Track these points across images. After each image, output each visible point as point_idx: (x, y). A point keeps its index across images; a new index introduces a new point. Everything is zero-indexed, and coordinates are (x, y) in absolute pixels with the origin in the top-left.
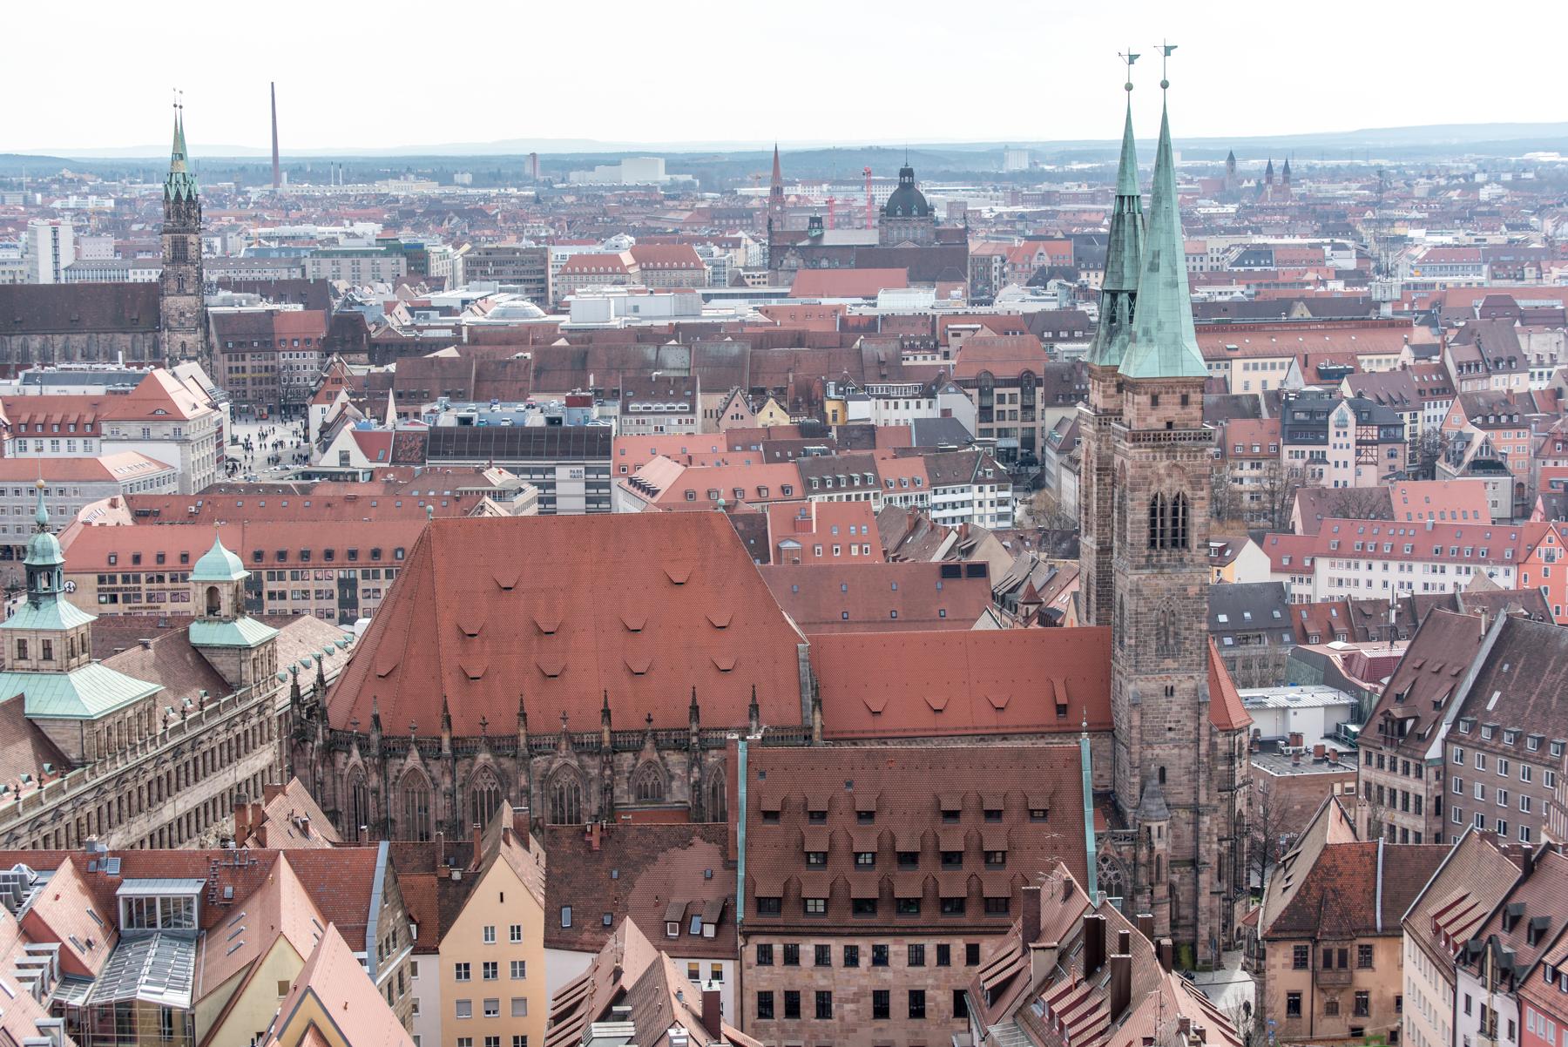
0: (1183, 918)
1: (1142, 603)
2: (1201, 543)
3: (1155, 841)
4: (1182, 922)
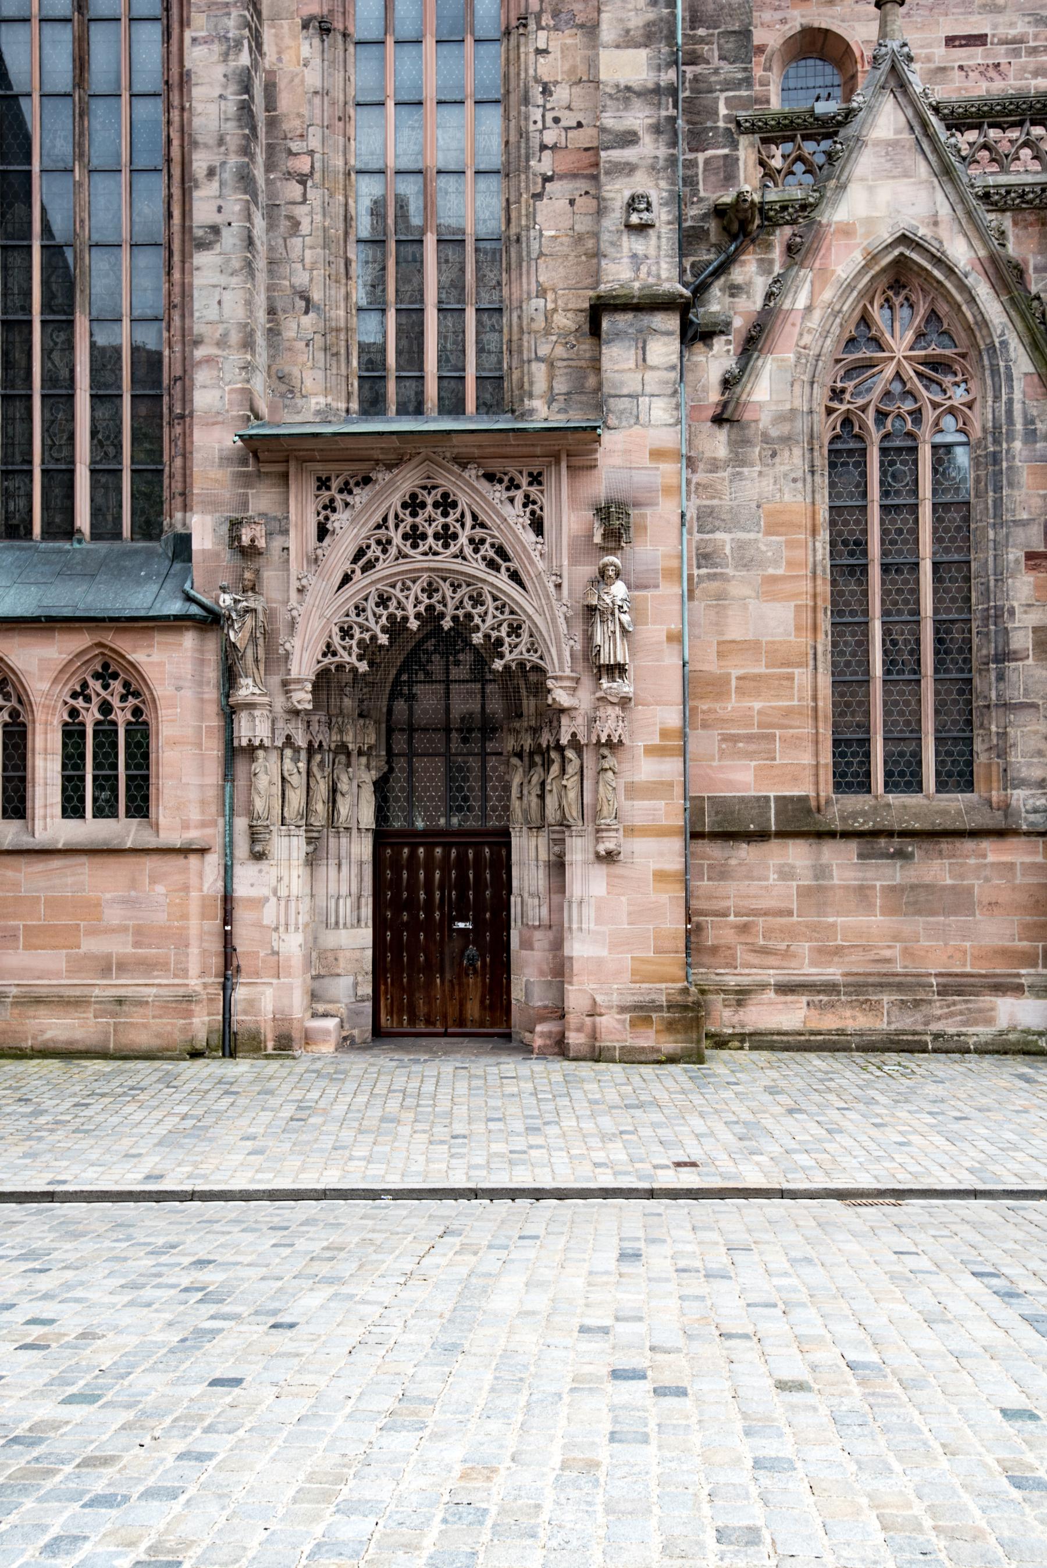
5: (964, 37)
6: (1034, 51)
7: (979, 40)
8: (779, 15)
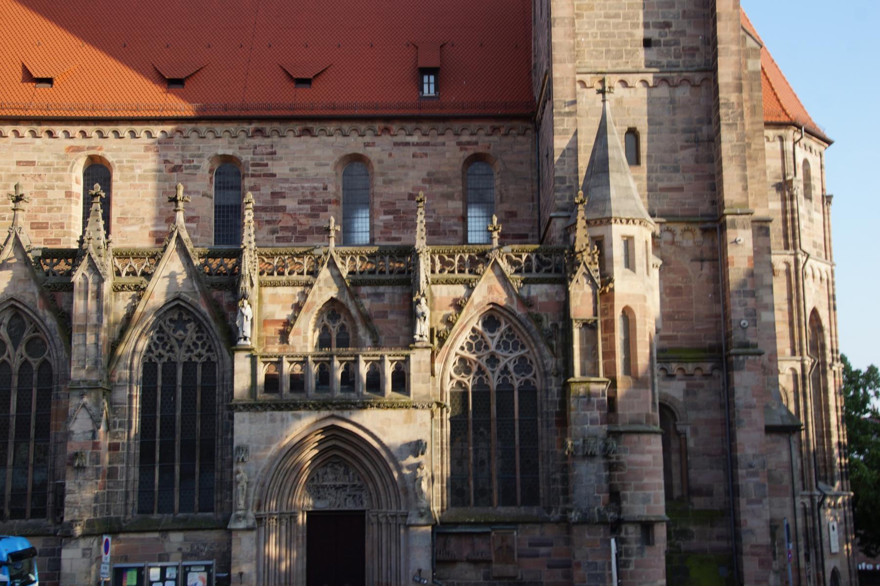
0: (699, 492)
3: (618, 269)
4: (699, 502)
5: (25, 162)
6: (56, 170)
7: (32, 163)
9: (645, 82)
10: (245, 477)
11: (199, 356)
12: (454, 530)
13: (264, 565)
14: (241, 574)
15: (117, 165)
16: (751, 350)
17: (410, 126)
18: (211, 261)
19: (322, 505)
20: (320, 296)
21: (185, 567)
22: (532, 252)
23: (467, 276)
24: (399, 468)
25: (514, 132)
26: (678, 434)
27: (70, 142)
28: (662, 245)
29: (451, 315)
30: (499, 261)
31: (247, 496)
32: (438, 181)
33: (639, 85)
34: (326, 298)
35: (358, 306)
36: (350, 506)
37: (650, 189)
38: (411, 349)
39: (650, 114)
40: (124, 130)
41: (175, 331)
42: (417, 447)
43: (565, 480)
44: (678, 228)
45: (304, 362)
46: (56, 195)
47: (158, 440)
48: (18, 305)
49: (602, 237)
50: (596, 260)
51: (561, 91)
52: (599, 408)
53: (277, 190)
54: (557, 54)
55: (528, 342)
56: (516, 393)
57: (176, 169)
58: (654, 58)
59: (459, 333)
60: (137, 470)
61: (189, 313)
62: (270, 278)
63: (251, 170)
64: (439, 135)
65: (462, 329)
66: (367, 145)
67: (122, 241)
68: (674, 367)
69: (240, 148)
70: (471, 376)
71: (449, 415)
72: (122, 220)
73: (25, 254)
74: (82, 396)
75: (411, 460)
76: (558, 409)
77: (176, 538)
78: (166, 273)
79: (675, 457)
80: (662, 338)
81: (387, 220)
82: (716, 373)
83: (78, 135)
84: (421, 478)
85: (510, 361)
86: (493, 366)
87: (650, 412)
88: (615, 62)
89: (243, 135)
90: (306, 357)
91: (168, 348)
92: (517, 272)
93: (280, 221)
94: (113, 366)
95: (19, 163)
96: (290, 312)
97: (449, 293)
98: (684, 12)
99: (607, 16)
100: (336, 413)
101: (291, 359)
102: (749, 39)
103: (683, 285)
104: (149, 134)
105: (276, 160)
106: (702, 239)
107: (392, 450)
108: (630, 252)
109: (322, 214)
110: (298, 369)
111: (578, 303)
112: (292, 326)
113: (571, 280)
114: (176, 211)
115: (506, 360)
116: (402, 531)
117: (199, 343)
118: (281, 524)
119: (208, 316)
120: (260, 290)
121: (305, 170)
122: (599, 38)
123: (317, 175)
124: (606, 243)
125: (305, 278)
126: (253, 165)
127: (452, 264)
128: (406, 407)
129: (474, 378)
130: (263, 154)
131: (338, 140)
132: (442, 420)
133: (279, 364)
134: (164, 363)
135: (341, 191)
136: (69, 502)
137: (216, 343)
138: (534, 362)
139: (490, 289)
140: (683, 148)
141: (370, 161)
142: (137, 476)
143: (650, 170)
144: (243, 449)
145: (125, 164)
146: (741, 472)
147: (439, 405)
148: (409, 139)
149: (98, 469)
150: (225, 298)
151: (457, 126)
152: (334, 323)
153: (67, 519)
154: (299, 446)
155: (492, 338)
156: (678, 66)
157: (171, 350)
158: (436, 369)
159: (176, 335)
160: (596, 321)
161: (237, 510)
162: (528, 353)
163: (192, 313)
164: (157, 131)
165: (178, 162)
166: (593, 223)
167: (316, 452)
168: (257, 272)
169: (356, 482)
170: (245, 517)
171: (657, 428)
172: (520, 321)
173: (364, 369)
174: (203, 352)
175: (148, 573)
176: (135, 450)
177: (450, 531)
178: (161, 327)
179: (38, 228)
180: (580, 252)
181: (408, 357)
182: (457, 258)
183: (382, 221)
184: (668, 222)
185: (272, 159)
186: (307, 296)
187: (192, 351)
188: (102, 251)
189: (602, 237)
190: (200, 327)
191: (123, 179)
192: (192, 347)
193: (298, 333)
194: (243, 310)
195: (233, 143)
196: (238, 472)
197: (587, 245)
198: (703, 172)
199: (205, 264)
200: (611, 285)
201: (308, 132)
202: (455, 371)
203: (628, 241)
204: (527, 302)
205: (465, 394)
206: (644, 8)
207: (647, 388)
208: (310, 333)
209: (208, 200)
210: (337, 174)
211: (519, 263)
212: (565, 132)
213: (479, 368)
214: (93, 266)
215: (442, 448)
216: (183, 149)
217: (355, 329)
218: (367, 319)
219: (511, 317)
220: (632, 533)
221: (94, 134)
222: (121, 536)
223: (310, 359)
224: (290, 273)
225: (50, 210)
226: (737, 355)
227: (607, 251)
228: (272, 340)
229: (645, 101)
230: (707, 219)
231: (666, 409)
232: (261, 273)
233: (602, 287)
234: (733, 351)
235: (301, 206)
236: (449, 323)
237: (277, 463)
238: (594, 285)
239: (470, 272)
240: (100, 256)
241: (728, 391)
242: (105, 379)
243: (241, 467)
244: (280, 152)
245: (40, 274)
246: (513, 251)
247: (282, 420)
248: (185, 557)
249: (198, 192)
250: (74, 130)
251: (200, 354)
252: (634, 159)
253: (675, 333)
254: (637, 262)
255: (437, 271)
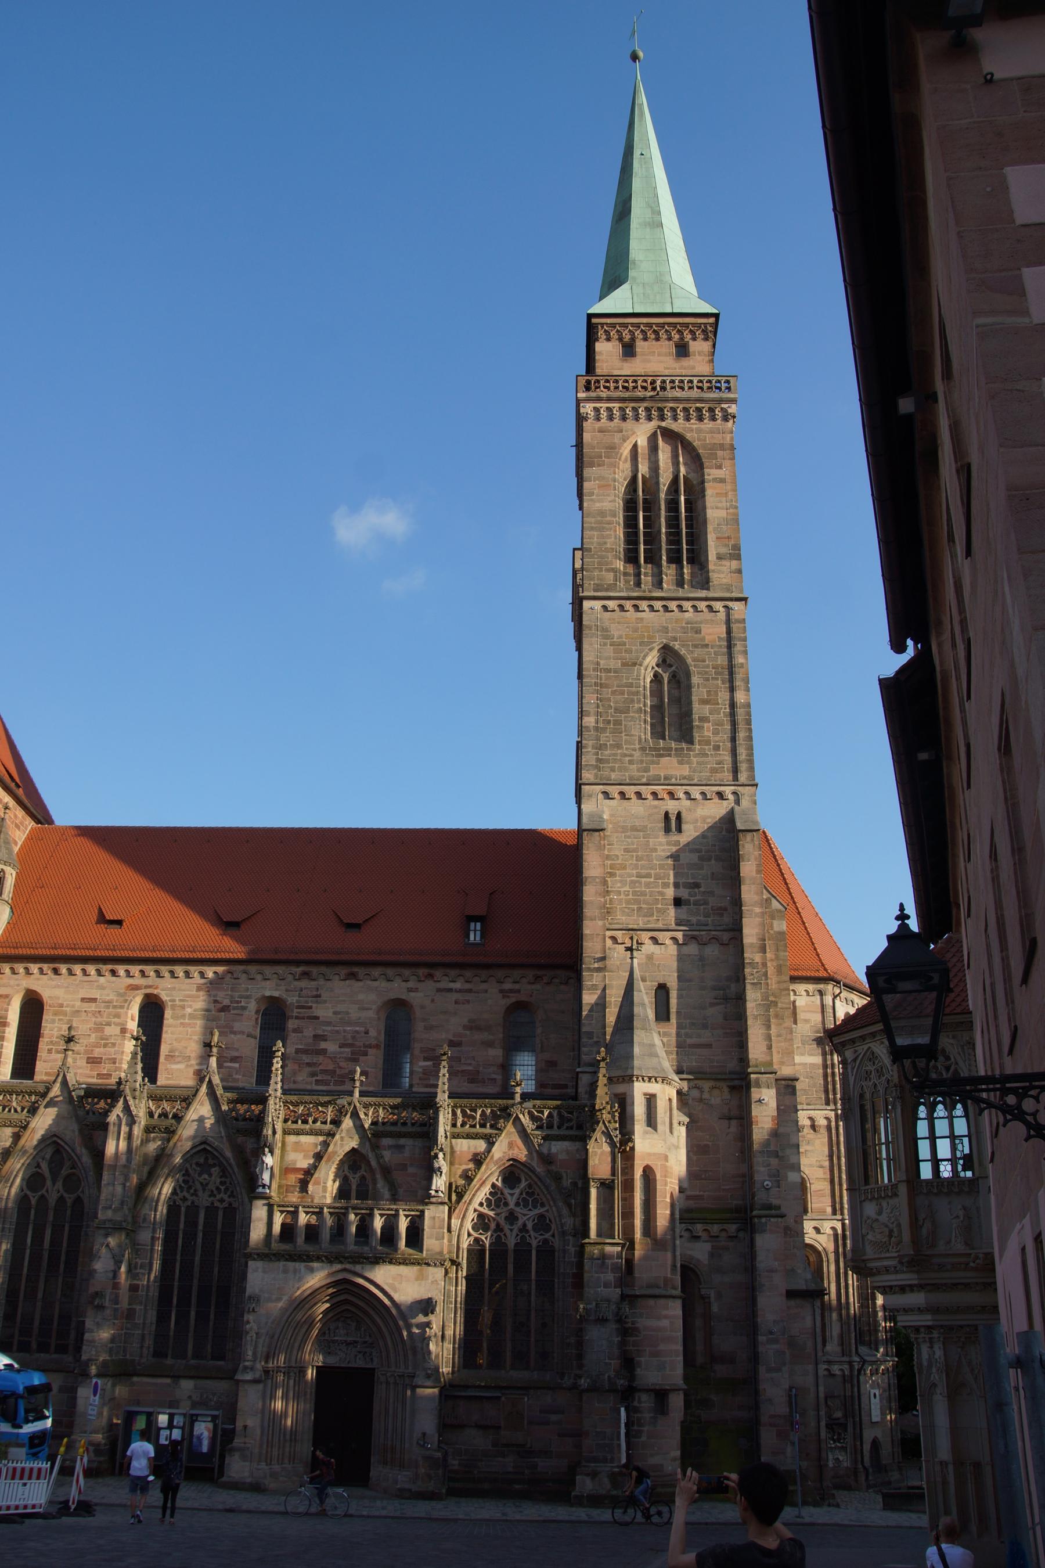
1: (609, 650)
2: (723, 550)
3: (639, 1128)
6: (115, 1007)
7: (94, 1000)
8: (17, 982)
9: (674, 939)
10: (255, 1327)
11: (222, 1201)
12: (463, 1394)
13: (273, 1420)
14: (245, 1427)
15: (170, 1003)
16: (773, 1212)
17: (453, 973)
18: (239, 1106)
19: (333, 1361)
20: (342, 1146)
21: (192, 1415)
22: (554, 1108)
23: (488, 1130)
24: (409, 1327)
25: (556, 981)
26: (703, 1297)
27: (130, 981)
28: (690, 1102)
29: (470, 1170)
30: (521, 1116)
31: (256, 1347)
32: (479, 1028)
33: (668, 942)
34: (347, 1149)
35: (379, 1157)
36: (360, 1363)
37: (679, 1046)
38: (427, 1204)
39: (680, 970)
40: (179, 970)
41: (200, 1175)
42: (427, 1306)
43: (580, 1344)
44: (706, 1085)
45: (319, 1213)
46: (112, 1031)
47: (176, 1284)
48: (59, 1141)
49: (625, 1094)
50: (617, 1119)
51: (591, 948)
52: (612, 1271)
53: (320, 1032)
54: (588, 911)
55: (547, 1200)
56: (534, 1253)
57: (225, 1009)
58: (684, 917)
59: (478, 1189)
60: (155, 1313)
61: (214, 1157)
62: (294, 1126)
63: (296, 1012)
64: (482, 982)
65: (481, 1185)
66: (410, 990)
67: (168, 1079)
68: (699, 1227)
69: (287, 990)
70: (489, 1234)
71: (465, 1274)
72: (170, 1057)
73: (70, 1092)
74: (107, 1235)
75: (421, 1318)
76: (575, 1271)
77: (187, 1385)
78: (195, 1117)
79: (698, 1323)
80: (688, 1198)
81: (427, 1066)
82: (741, 1234)
83: (137, 974)
84: (430, 1337)
85: (528, 1219)
86: (512, 1224)
87: (669, 1276)
88: (646, 919)
89: (290, 977)
90: (322, 1209)
91: (192, 1191)
92: (538, 1128)
93: (320, 1064)
94: (139, 1207)
95: (83, 1000)
96: (312, 1161)
97: (469, 1148)
98: (713, 874)
99: (639, 876)
100: (348, 1266)
101: (307, 1210)
102: (774, 901)
103: (710, 1143)
104: (202, 975)
105: (319, 1003)
106: (729, 1097)
107: (402, 1308)
108: (652, 1109)
109: (361, 1058)
110: (313, 1220)
111: (597, 1162)
112: (312, 1175)
113: (590, 1138)
114: (210, 1056)
115: (525, 1218)
116: (409, 1393)
117: (223, 1188)
118: (289, 1379)
119: (232, 1161)
120: (283, 1138)
121: (347, 1013)
122: (631, 897)
123: (360, 1018)
124: (628, 1101)
125: (328, 1127)
126: (298, 1007)
127: (474, 1118)
128: (419, 1264)
129: (492, 1236)
130: (308, 997)
131: (382, 984)
132: (457, 1278)
133: (295, 1214)
134: (188, 1206)
135: (383, 1036)
136: (87, 1341)
137: (238, 1189)
138: (553, 1221)
139: (511, 1145)
140: (712, 1005)
141: (412, 1006)
142: (154, 1319)
143: (679, 1027)
144: (255, 1299)
145: (177, 1003)
146: (761, 1339)
147: (453, 1262)
148: (452, 985)
149: (116, 1310)
150: (250, 1144)
151: (500, 973)
152: (355, 1173)
153: (84, 1357)
154: (313, 1297)
155: (512, 1195)
156: (707, 925)
157: (195, 1194)
158: (452, 1225)
159: (201, 1179)
160: (613, 1181)
161: (245, 1361)
162: (547, 1211)
163: (217, 1157)
164: (210, 972)
165: (226, 1002)
166: (615, 1080)
167: (328, 1305)
168: (282, 1117)
169: (367, 1339)
170: (252, 1369)
171: (678, 1292)
172: (539, 1179)
173: (378, 1223)
174: (225, 1197)
175: (157, 1419)
176: (154, 1292)
177: (459, 1394)
178: (187, 1170)
179: (93, 1063)
180: (600, 1110)
181: (423, 1212)
182: (479, 1112)
183: (421, 1067)
184: (696, 1079)
185: (317, 1002)
186: (329, 1145)
187: (215, 1196)
188: (137, 1093)
189: (625, 1094)
190: (224, 1172)
191: (175, 1017)
192: (215, 1192)
193: (317, 1183)
194: (264, 1158)
195: (281, 985)
196: (248, 1322)
197: (607, 1103)
198: (731, 1029)
199: (231, 1110)
200: (630, 1144)
201: (353, 976)
202: (473, 1228)
203: (651, 1100)
204: (547, 1159)
205: (483, 1251)
206: (674, 869)
207: (666, 1251)
208: (330, 1183)
209: (252, 1040)
210: (379, 1018)
211: (542, 1119)
212: (594, 987)
213: (498, 1225)
214: (127, 1109)
215: (456, 1307)
216: (233, 989)
217: (375, 1182)
218: (386, 1171)
219: (530, 1174)
220: (645, 1402)
221: (152, 974)
222: (135, 1379)
223: (326, 1210)
224: (314, 1122)
225: (105, 1046)
226: (760, 1217)
227: (628, 1108)
228: (292, 1189)
229: (675, 958)
230: (734, 1076)
231: (688, 1272)
232: (286, 1121)
233: (621, 1145)
234: (755, 1213)
235: (342, 1050)
236: (468, 1178)
237: (288, 1313)
238: (612, 1144)
239: (492, 1127)
240: (134, 1098)
241: (751, 1254)
242: (130, 1219)
243: (251, 1317)
244: (325, 995)
245: (81, 1113)
246: (534, 1106)
247: (295, 1271)
248: (194, 1405)
249: (243, 1033)
250: (135, 969)
251: (222, 1198)
252: (662, 1014)
253: (701, 1193)
254: (659, 1120)
255: (459, 1124)
